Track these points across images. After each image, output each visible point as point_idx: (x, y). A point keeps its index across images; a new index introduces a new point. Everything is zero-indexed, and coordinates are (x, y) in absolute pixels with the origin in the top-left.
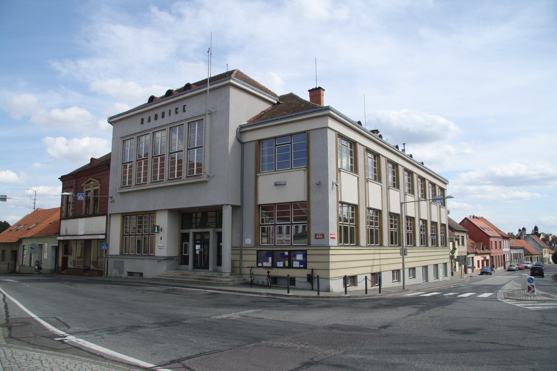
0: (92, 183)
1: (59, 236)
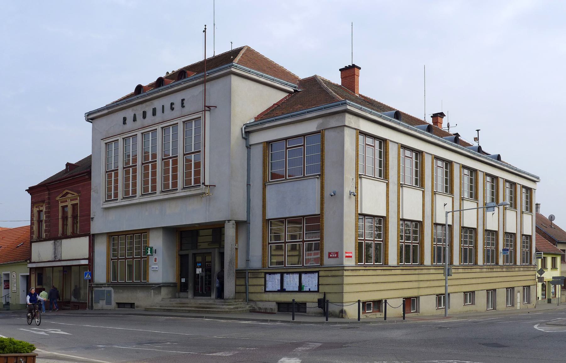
0: (69, 195)
1: (31, 262)
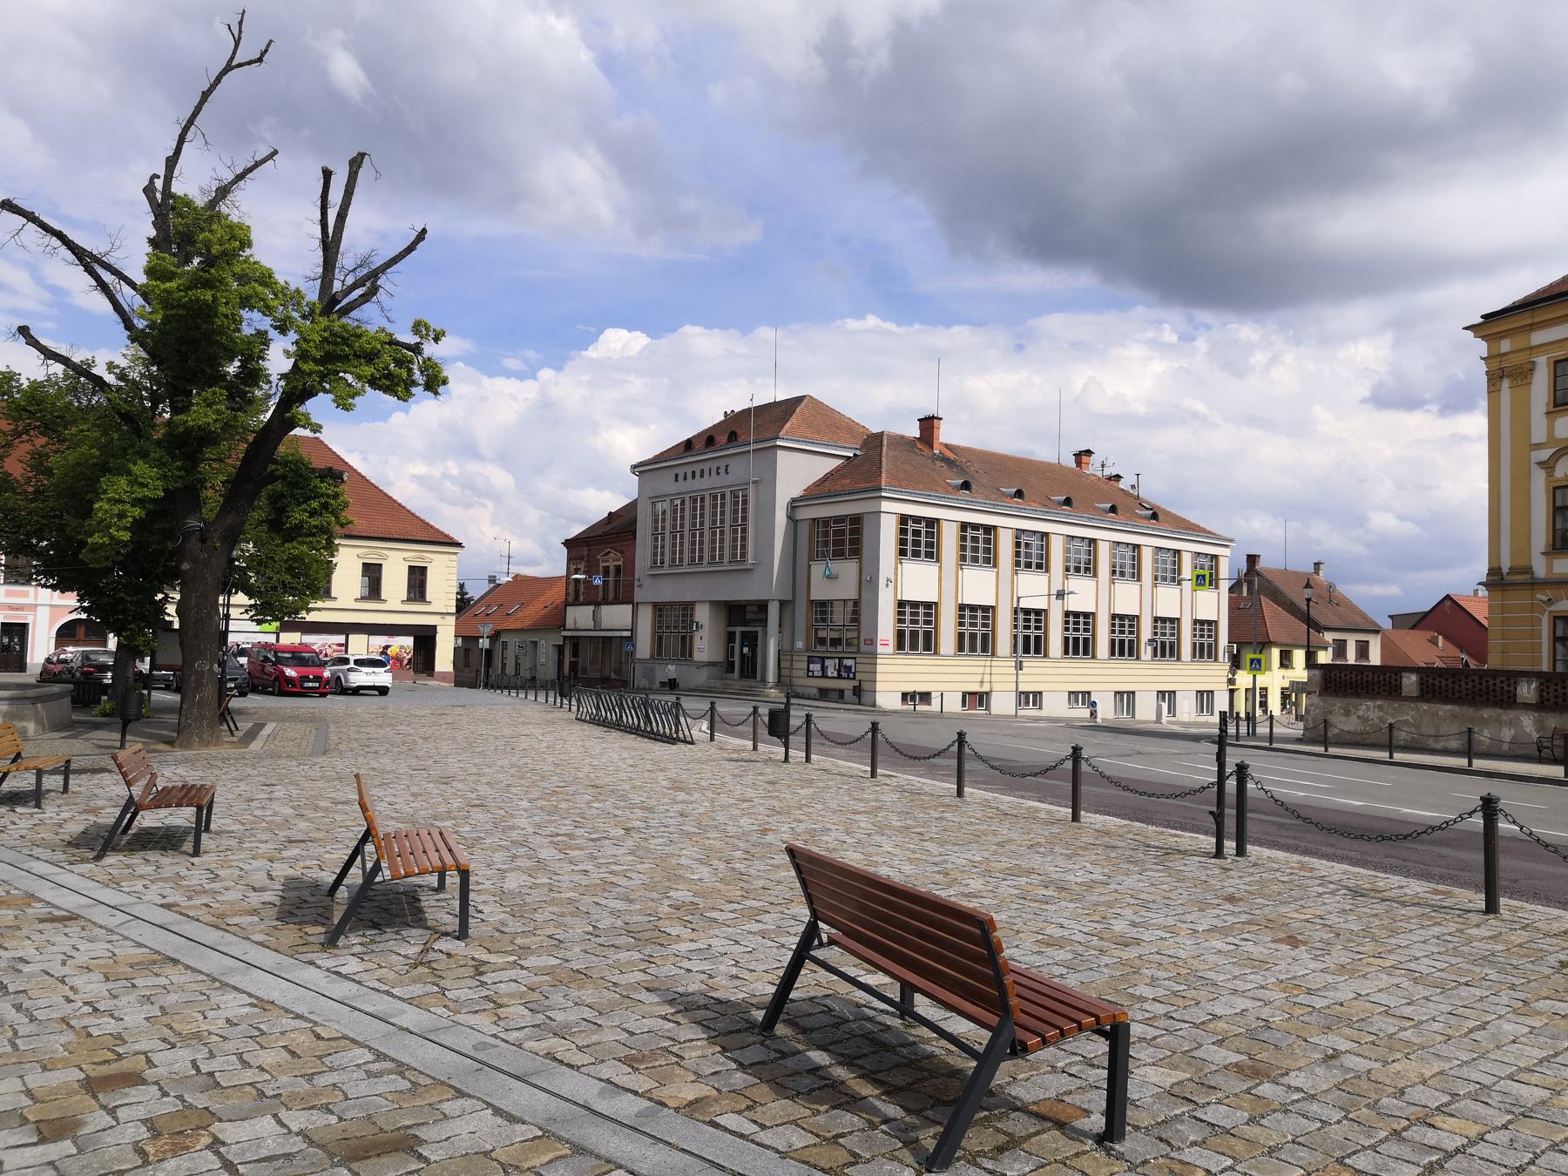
0: (611, 555)
1: (565, 630)
